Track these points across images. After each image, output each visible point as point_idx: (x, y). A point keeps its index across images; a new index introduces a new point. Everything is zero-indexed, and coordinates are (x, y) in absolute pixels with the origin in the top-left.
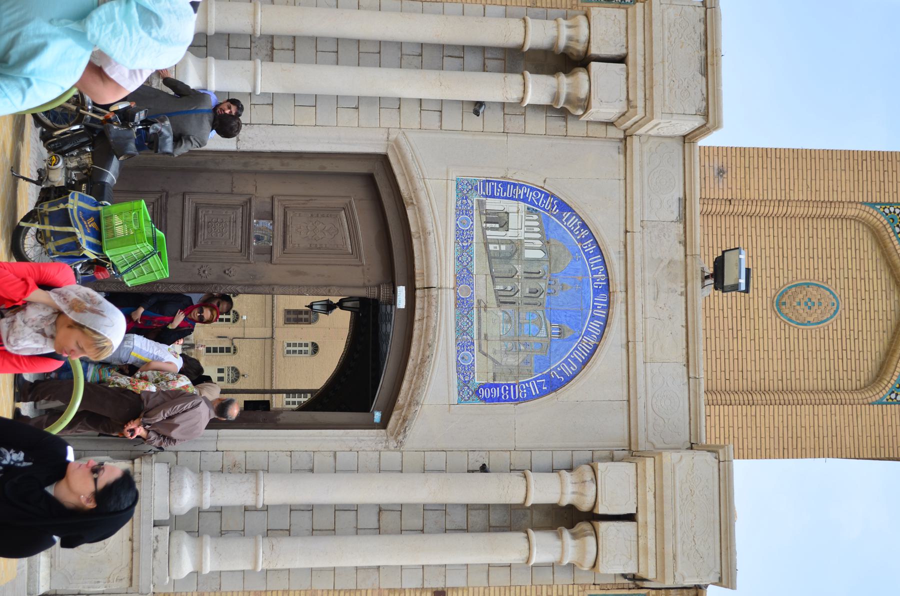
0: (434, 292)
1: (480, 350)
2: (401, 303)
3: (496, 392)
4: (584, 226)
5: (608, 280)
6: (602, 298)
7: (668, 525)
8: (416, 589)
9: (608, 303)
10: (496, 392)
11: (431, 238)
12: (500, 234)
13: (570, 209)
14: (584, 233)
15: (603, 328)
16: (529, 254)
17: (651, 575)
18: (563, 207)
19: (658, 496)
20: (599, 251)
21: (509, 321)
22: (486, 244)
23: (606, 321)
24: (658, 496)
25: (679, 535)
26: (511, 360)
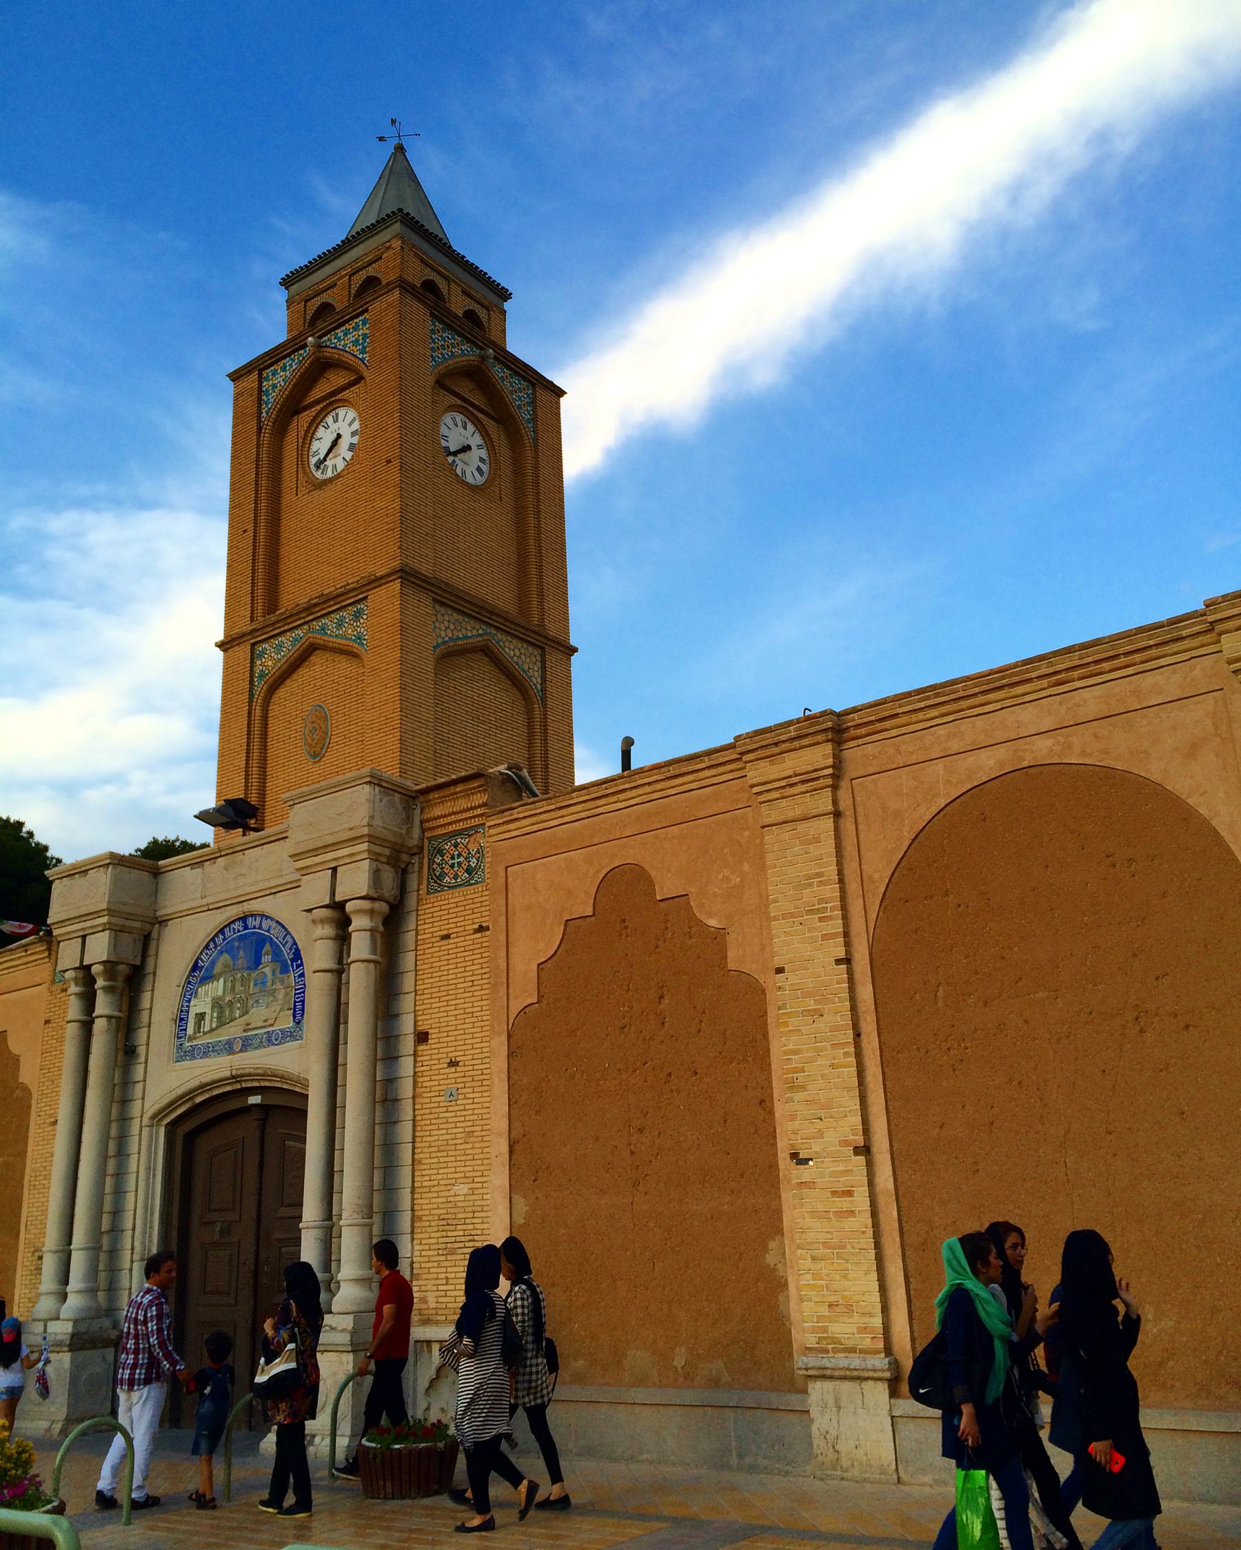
0: (234, 1072)
1: (272, 1025)
2: (255, 1100)
3: (299, 1006)
4: (207, 947)
5: (239, 919)
6: (250, 921)
7: (330, 840)
8: (415, 1061)
9: (252, 915)
10: (299, 1006)
11: (204, 1080)
12: (208, 1018)
13: (196, 963)
14: (212, 945)
15: (267, 917)
16: (220, 993)
17: (365, 846)
18: (195, 967)
19: (315, 851)
20: (222, 931)
21: (257, 1001)
22: (212, 1030)
23: (262, 916)
24: (315, 851)
25: (337, 829)
26: (280, 995)
